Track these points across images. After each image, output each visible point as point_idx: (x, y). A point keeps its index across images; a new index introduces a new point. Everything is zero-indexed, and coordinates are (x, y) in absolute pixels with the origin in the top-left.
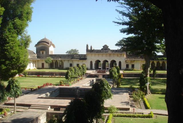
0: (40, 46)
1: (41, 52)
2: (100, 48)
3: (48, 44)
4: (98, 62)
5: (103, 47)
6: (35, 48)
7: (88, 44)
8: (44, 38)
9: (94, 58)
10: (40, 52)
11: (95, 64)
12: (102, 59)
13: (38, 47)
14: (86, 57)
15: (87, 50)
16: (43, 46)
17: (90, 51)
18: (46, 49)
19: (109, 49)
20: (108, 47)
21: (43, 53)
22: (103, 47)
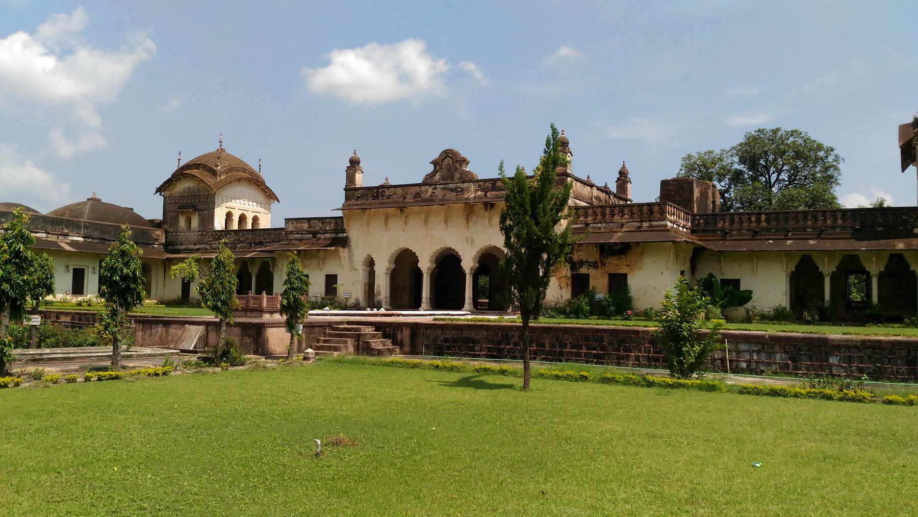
0: (182, 186)
1: (182, 222)
2: (414, 170)
3: (214, 173)
4: (405, 262)
5: (435, 163)
6: (159, 200)
7: (359, 155)
8: (213, 148)
9: (377, 243)
10: (177, 216)
11: (394, 275)
12: (426, 241)
13: (167, 193)
14: (343, 231)
15: (351, 190)
16: (189, 189)
17: (365, 199)
18: (202, 204)
19: (469, 178)
20: (464, 161)
21: (189, 221)
22: (435, 163)
